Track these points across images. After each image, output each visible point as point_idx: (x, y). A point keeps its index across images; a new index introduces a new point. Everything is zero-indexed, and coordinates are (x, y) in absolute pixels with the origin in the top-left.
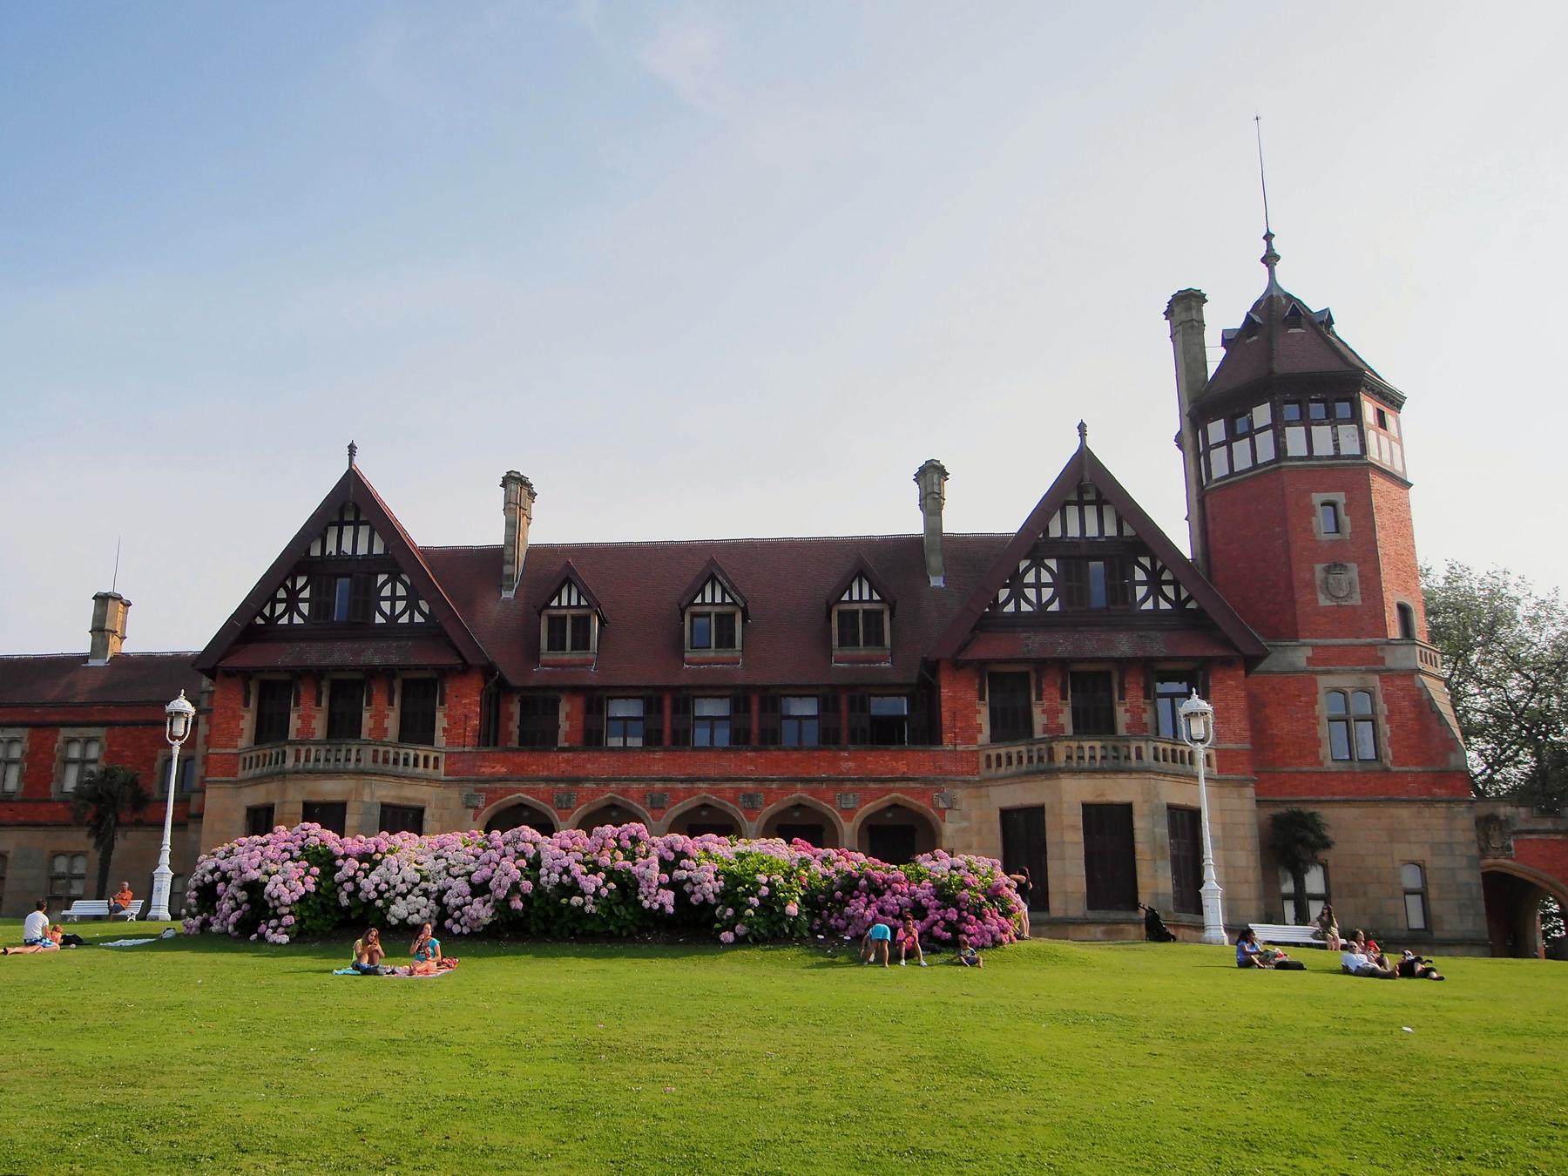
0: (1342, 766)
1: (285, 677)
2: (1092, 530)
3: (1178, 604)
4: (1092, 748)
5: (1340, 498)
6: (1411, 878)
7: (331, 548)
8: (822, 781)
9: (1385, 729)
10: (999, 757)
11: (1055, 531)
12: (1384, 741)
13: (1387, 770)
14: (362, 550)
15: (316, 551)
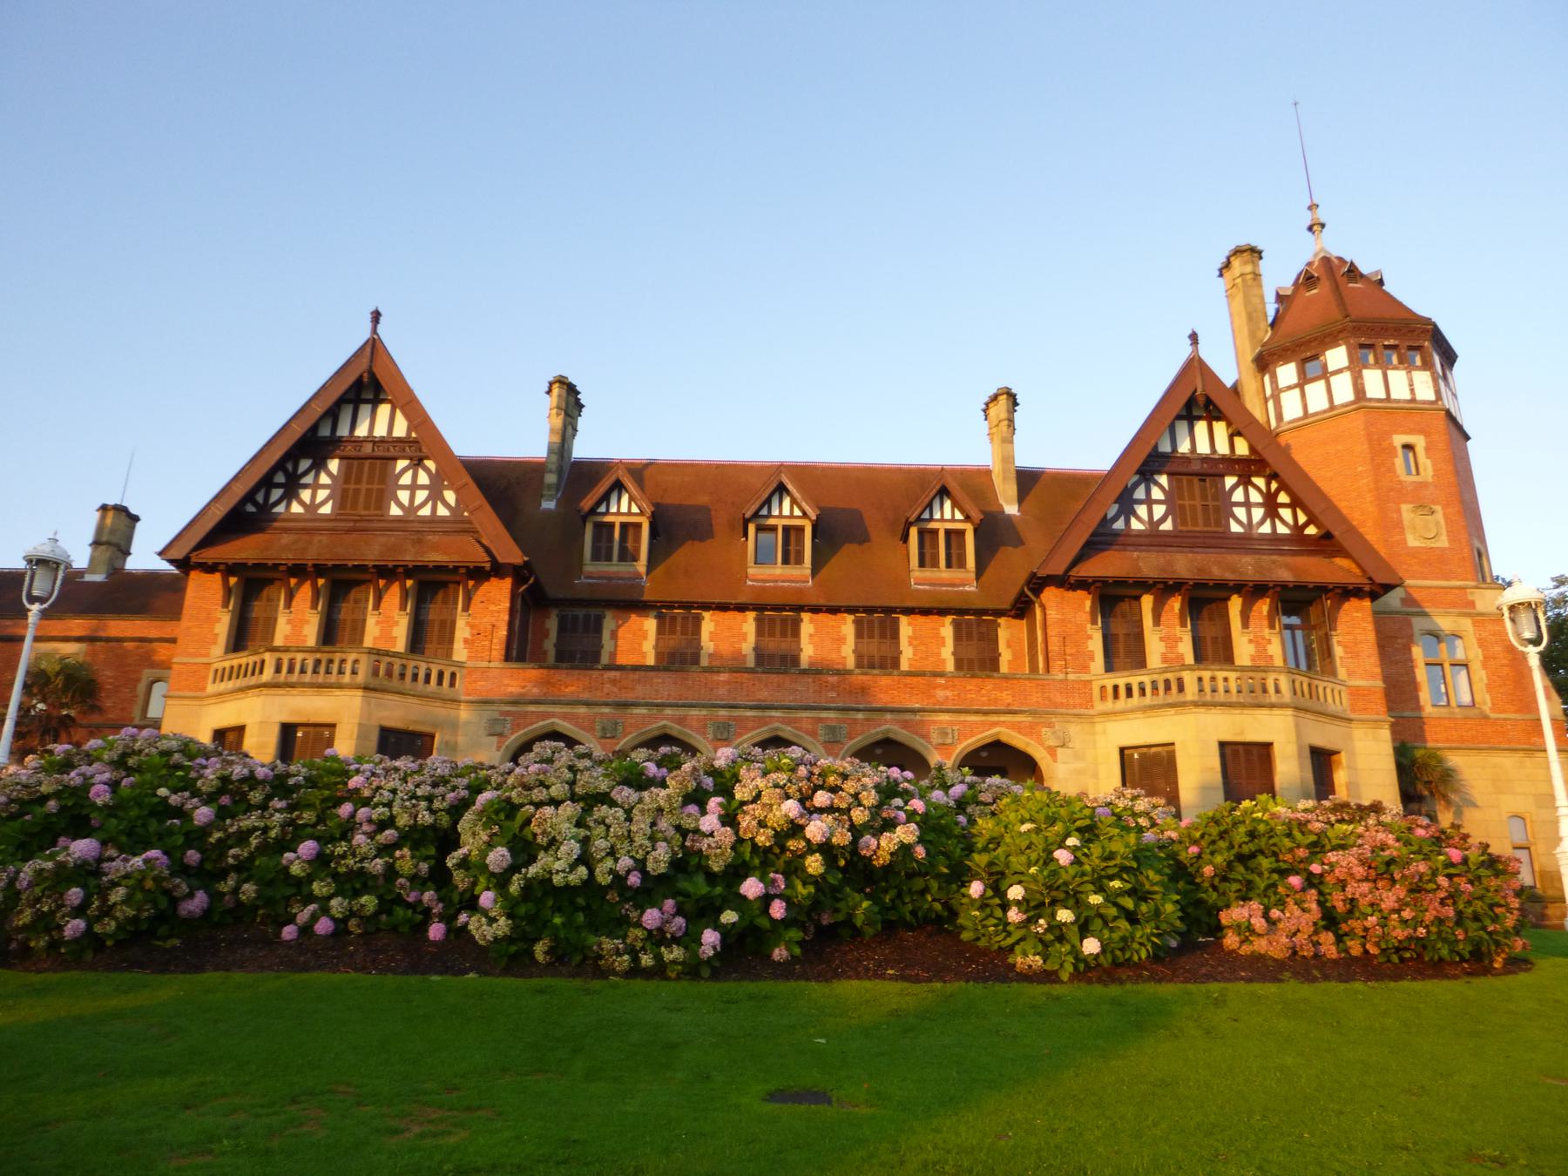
3: (1298, 529)
4: (1226, 679)
7: (343, 431)
9: (1480, 675)
10: (1116, 688)
12: (1480, 687)
13: (1486, 717)
15: (325, 432)
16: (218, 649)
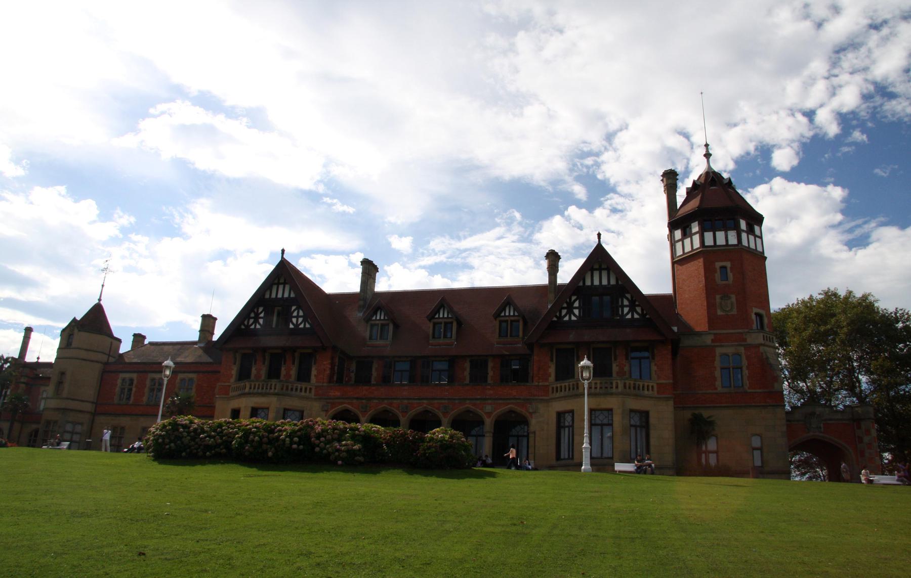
0: (725, 390)
1: (309, 351)
2: (605, 282)
3: (643, 315)
5: (728, 264)
6: (756, 442)
7: (273, 296)
8: (477, 399)
9: (746, 372)
11: (588, 283)
12: (745, 378)
14: (286, 295)
16: (232, 380)
